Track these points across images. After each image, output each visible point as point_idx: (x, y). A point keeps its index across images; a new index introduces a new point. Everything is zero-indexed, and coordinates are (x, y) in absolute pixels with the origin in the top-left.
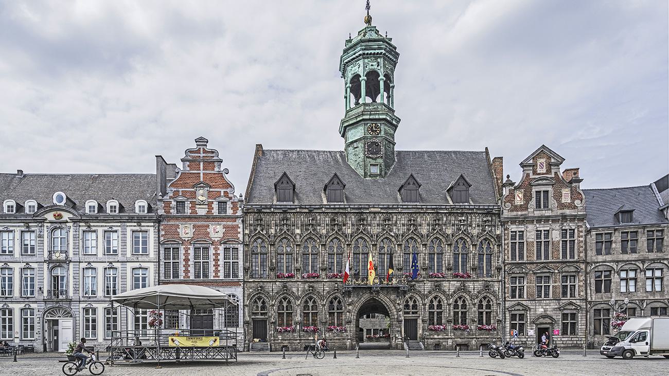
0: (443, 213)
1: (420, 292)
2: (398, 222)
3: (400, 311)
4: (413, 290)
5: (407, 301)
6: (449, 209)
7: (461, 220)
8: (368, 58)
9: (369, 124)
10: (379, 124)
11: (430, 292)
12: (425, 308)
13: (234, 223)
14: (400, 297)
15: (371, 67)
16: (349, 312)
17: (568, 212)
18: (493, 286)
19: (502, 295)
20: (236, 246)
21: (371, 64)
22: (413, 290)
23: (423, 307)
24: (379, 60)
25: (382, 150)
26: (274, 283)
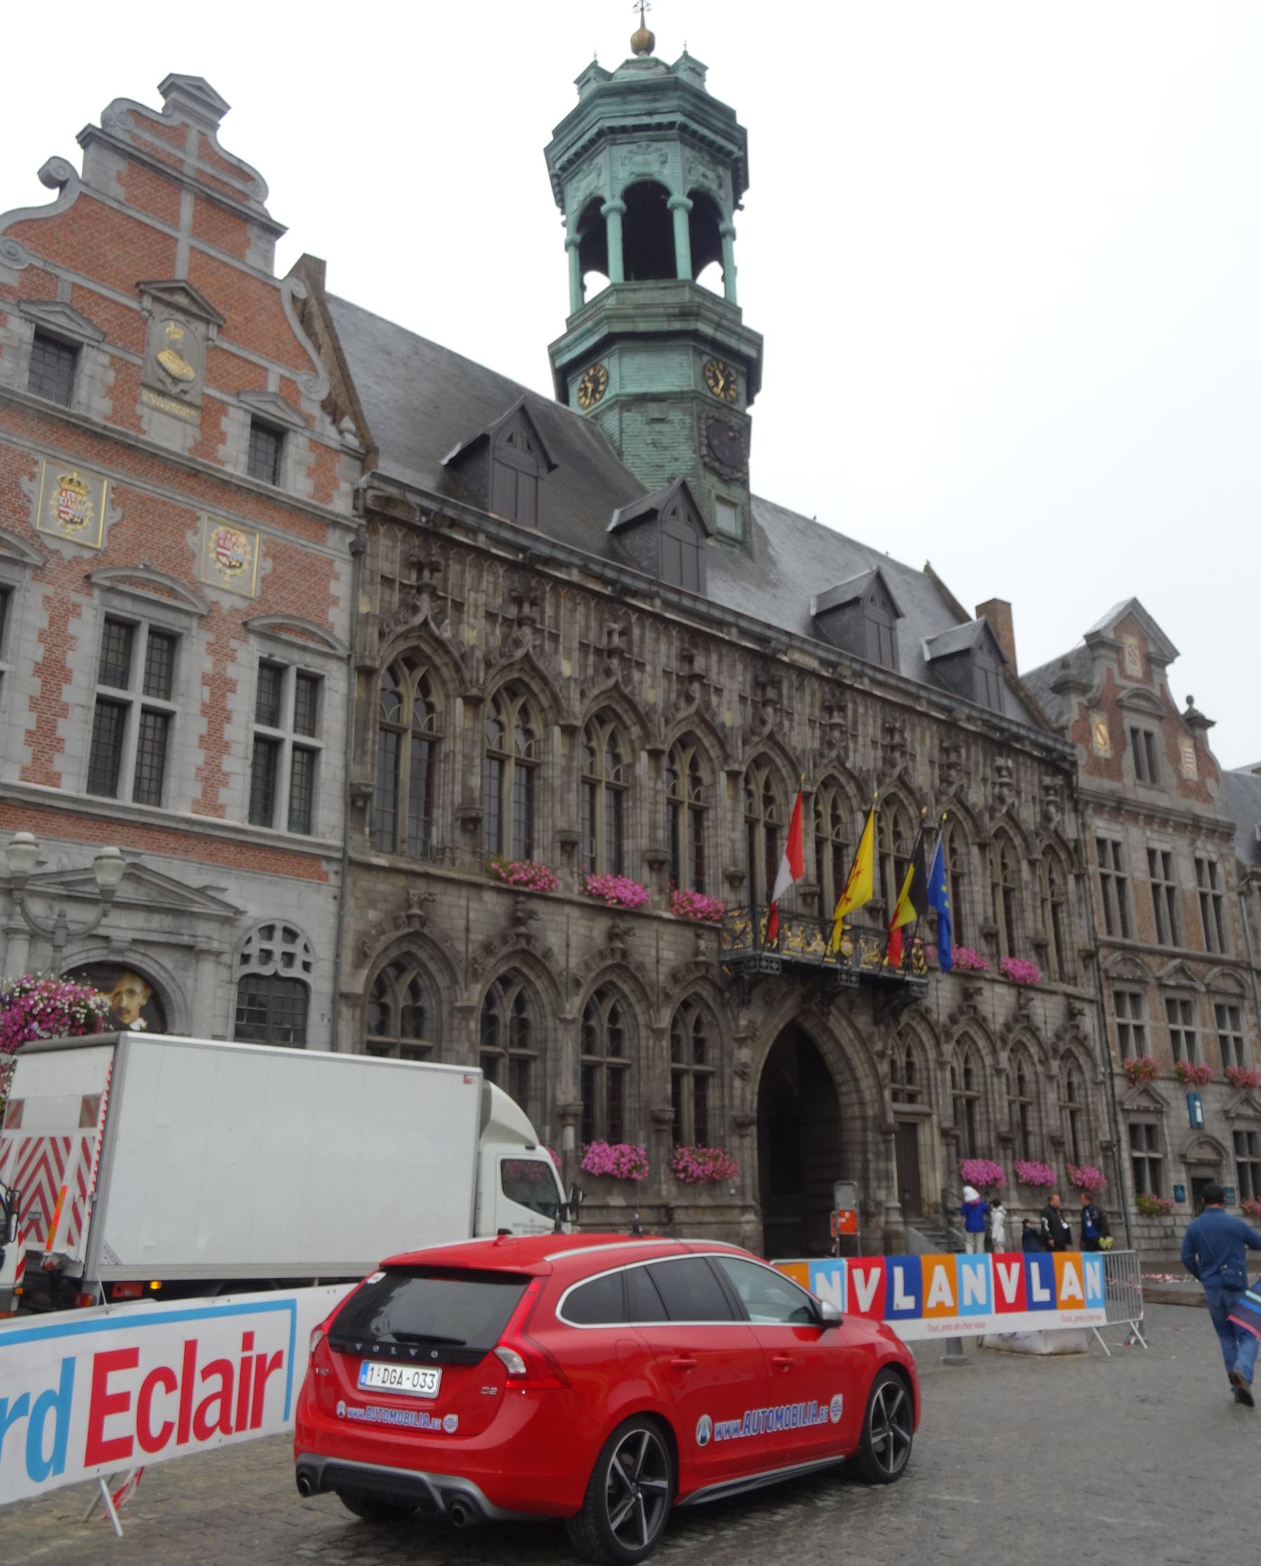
13: (315, 548)
17: (1199, 808)
20: (315, 665)
26: (473, 892)
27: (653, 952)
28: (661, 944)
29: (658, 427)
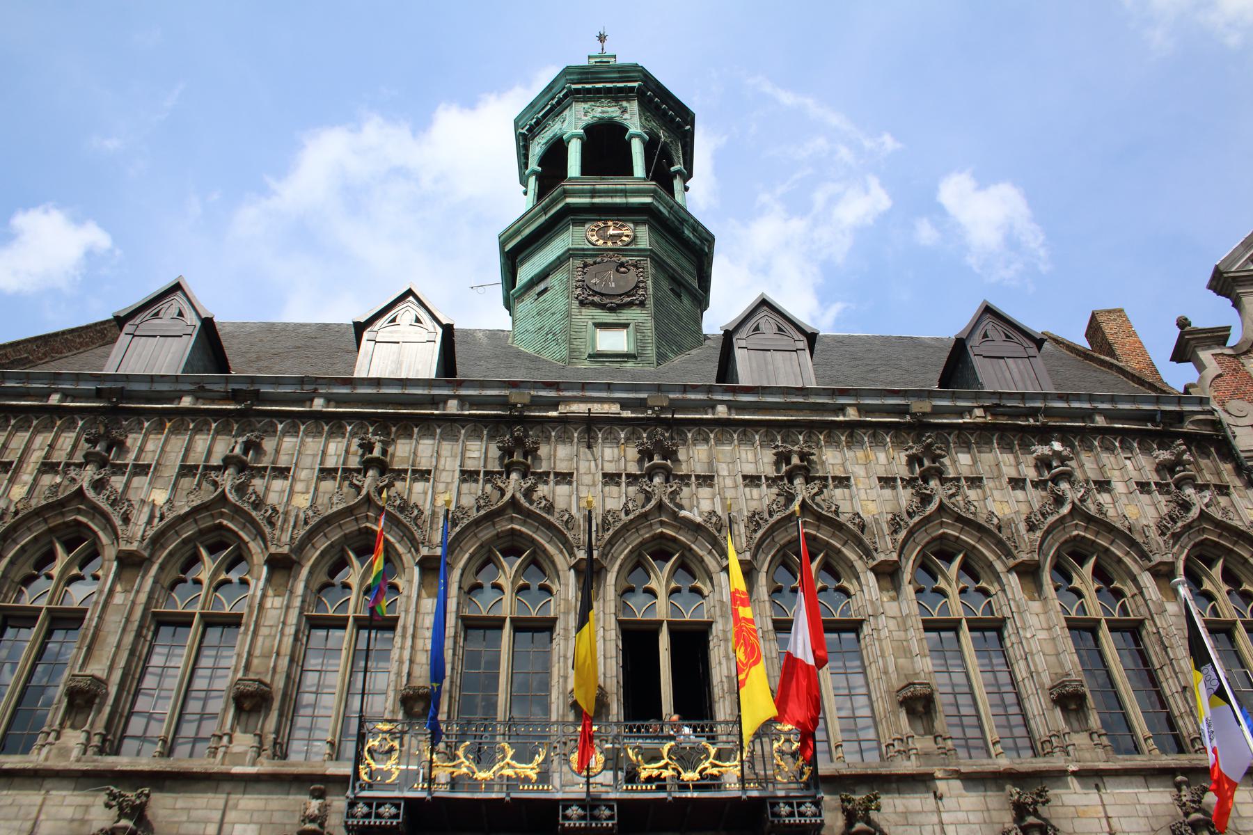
2: (723, 470)
8: (590, 100)
28: (231, 816)
29: (541, 299)
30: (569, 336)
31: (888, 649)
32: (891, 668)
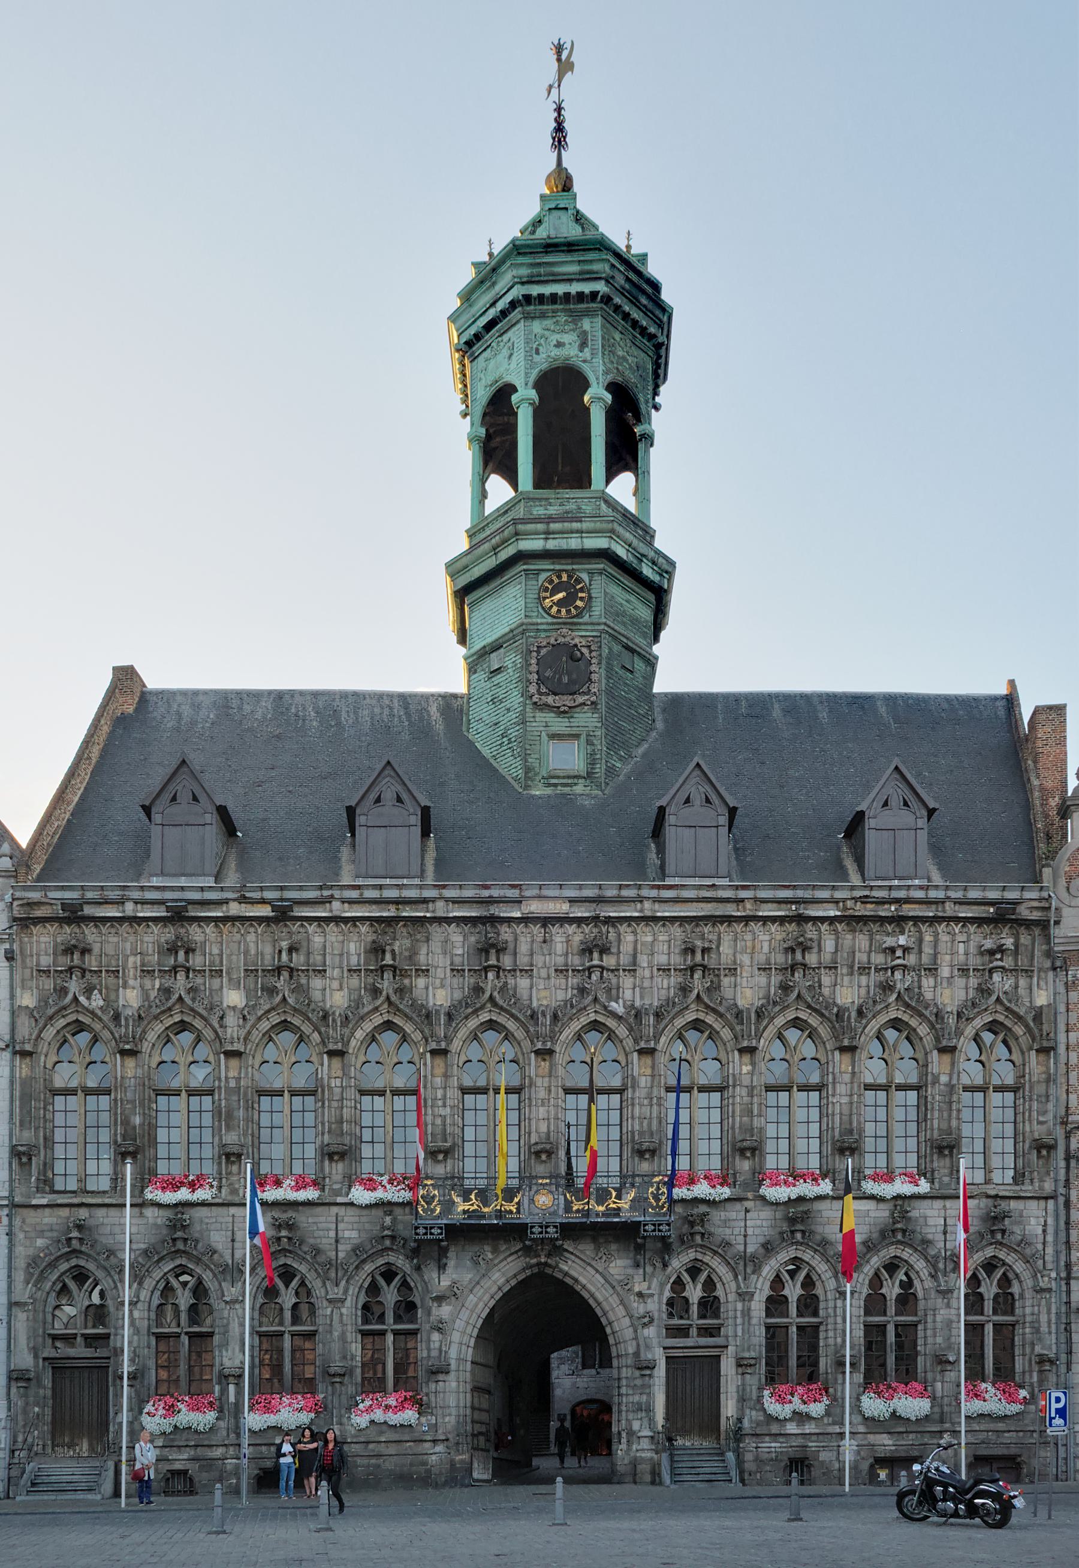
0: (823, 919)
1: (728, 1244)
3: (645, 1325)
4: (698, 1238)
5: (679, 1284)
6: (844, 900)
7: (892, 950)
9: (543, 576)
10: (585, 576)
11: (768, 1248)
12: (747, 1313)
14: (649, 1269)
15: (555, 352)
16: (439, 1330)
18: (1021, 1219)
19: (1057, 1252)
21: (554, 338)
22: (698, 1238)
23: (739, 1306)
24: (586, 324)
25: (594, 677)
27: (332, 1234)
28: (341, 1226)
30: (525, 749)
31: (738, 1113)
32: (737, 1125)
